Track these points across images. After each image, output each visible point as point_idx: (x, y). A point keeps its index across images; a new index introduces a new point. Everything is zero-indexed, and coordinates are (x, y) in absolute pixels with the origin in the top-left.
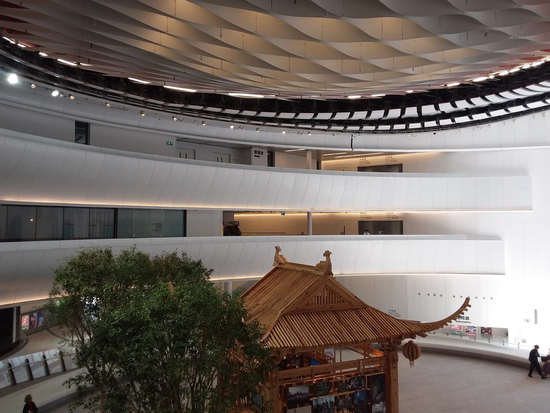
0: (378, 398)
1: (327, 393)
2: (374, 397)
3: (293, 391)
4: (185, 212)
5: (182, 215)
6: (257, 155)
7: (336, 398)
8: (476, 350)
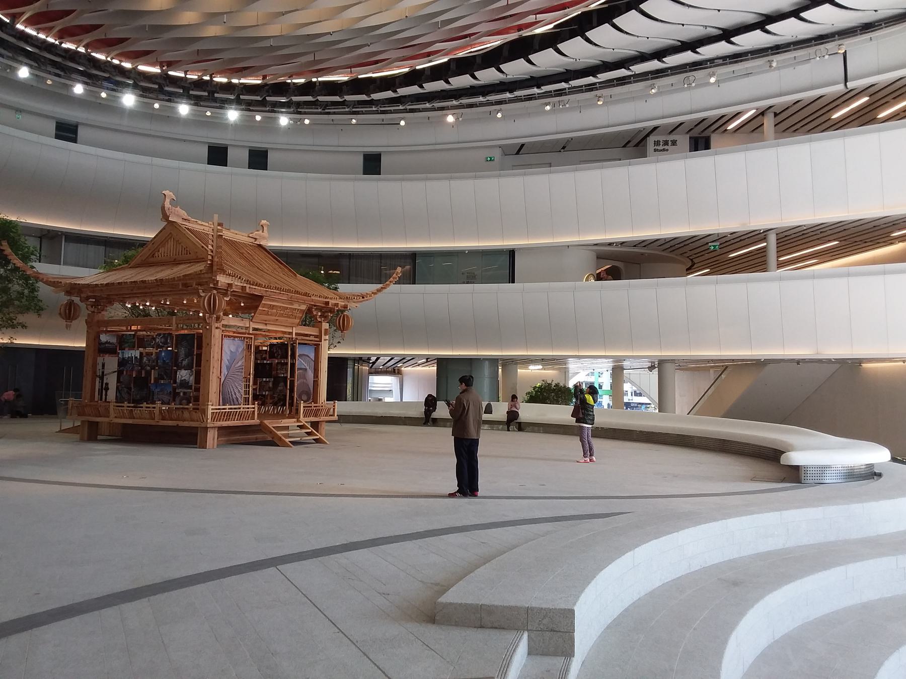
0: (185, 363)
1: (132, 347)
2: (180, 360)
3: (104, 338)
4: (512, 253)
5: (506, 258)
6: (661, 147)
7: (141, 354)
8: (765, 439)
